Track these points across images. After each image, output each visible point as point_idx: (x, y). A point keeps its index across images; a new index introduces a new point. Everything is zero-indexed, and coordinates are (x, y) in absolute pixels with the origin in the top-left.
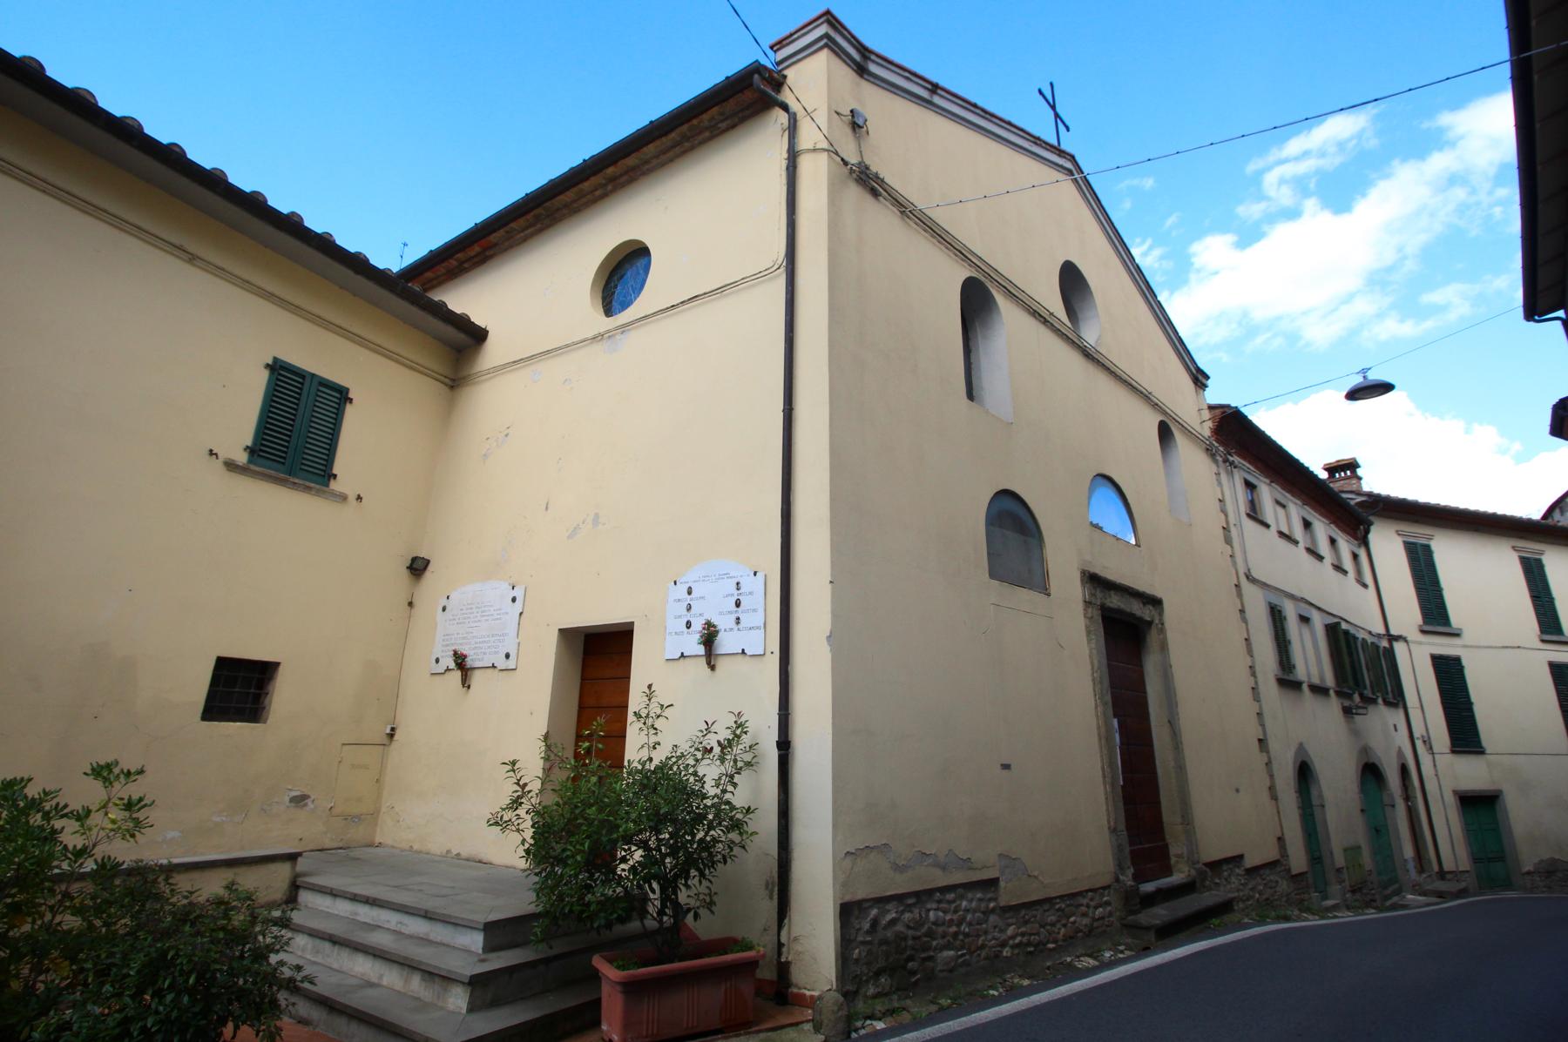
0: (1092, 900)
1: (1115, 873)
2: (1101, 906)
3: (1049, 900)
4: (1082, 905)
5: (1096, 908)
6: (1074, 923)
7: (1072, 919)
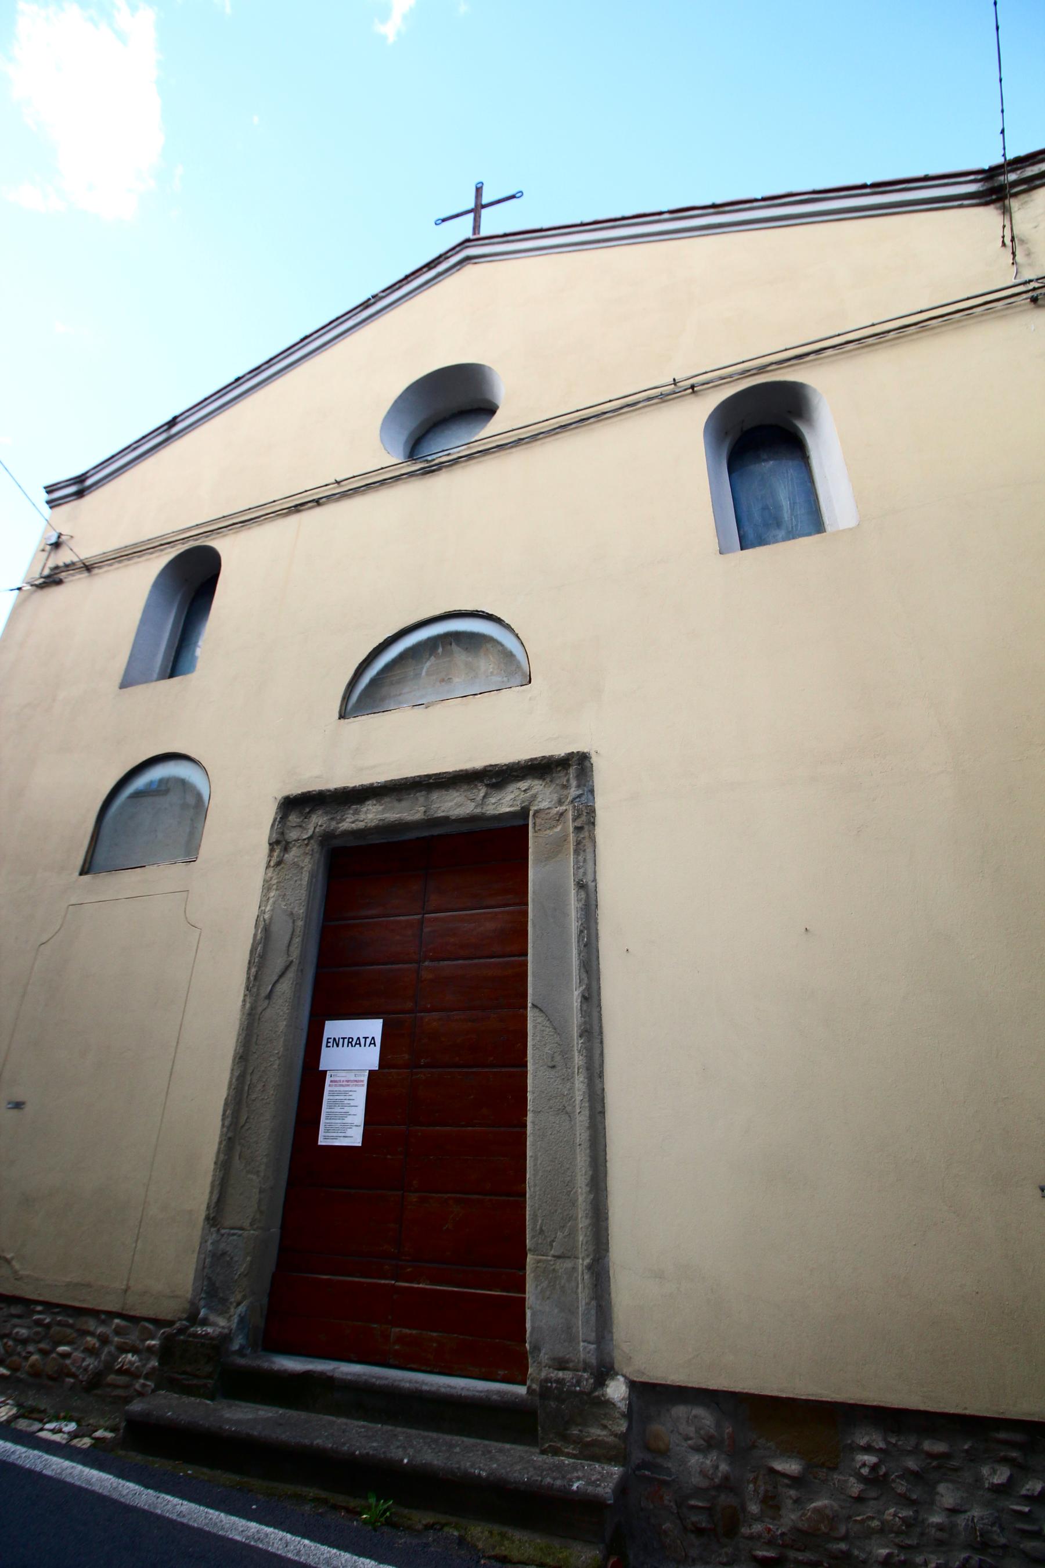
0: (118, 1332)
1: (192, 1303)
2: (135, 1351)
3: (27, 1303)
4: (92, 1334)
5: (123, 1349)
6: (65, 1355)
7: (62, 1349)
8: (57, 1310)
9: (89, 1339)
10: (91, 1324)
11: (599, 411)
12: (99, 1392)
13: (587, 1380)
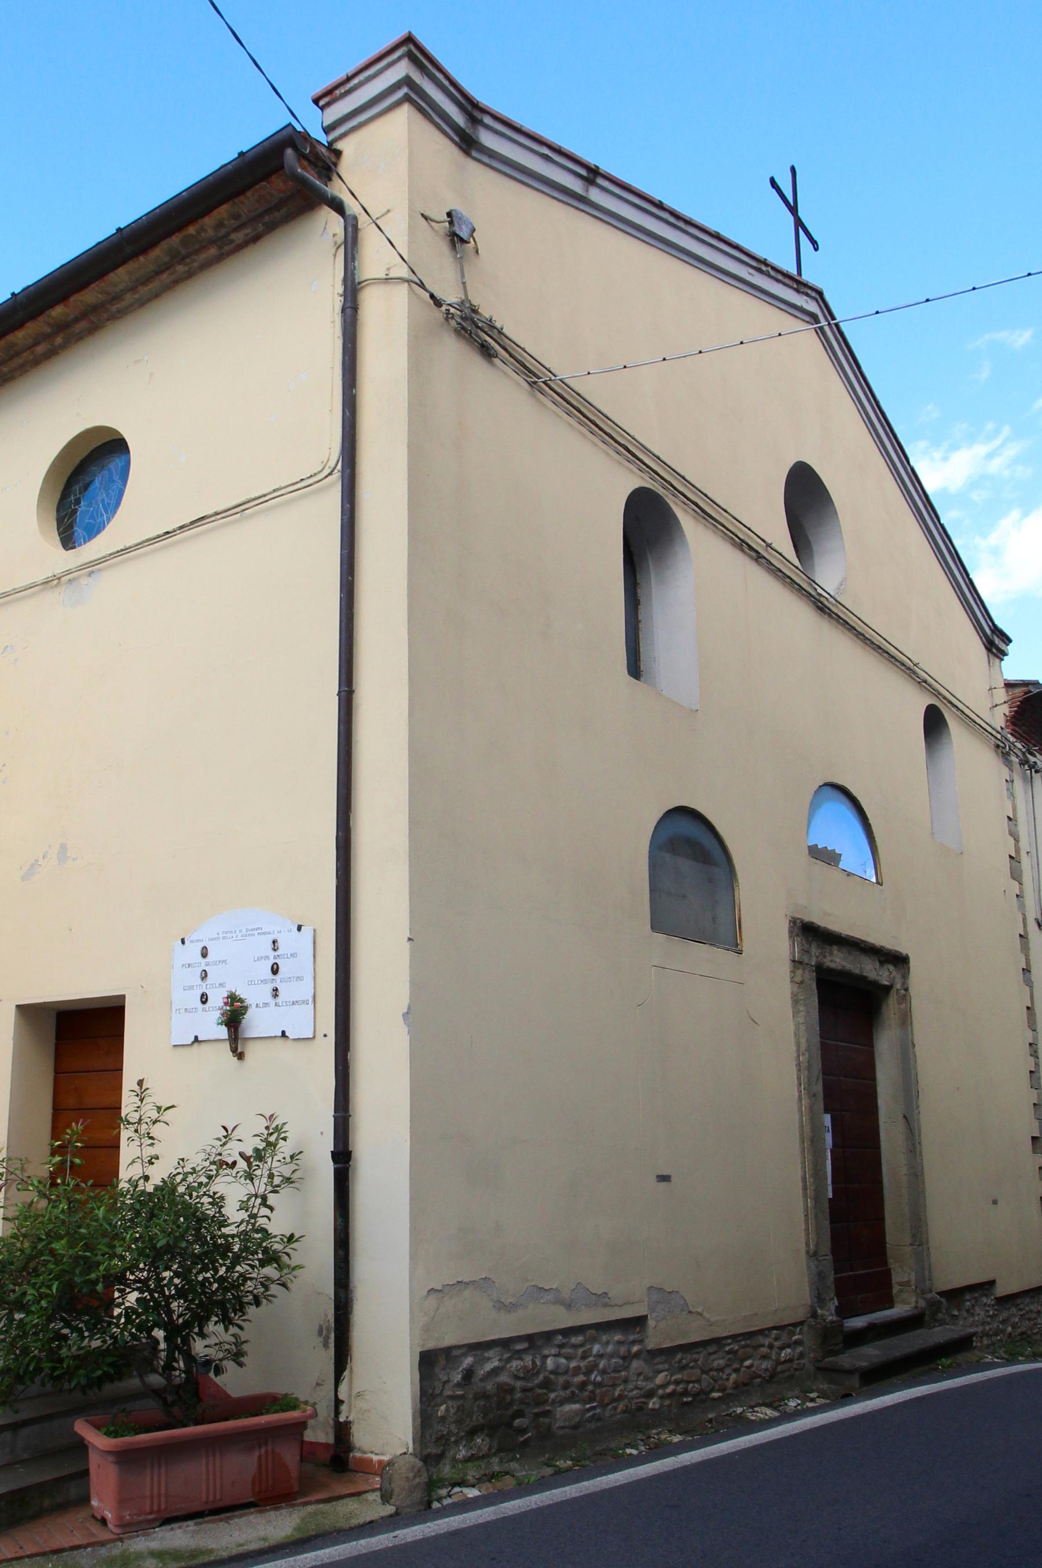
0: (776, 1339)
1: (812, 1307)
2: (789, 1346)
3: (718, 1341)
4: (762, 1346)
5: (782, 1348)
6: (751, 1366)
7: (747, 1363)
8: (740, 1338)
9: (762, 1349)
10: (761, 1340)
11: (887, 648)
12: (776, 1379)
13: (143, 1276)
